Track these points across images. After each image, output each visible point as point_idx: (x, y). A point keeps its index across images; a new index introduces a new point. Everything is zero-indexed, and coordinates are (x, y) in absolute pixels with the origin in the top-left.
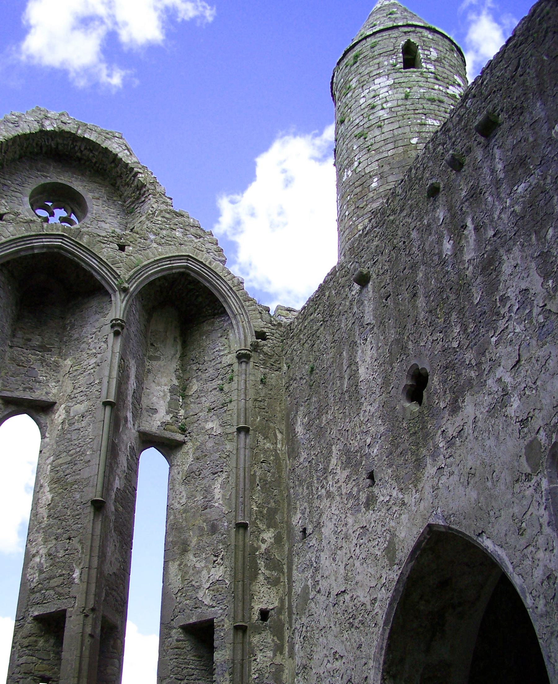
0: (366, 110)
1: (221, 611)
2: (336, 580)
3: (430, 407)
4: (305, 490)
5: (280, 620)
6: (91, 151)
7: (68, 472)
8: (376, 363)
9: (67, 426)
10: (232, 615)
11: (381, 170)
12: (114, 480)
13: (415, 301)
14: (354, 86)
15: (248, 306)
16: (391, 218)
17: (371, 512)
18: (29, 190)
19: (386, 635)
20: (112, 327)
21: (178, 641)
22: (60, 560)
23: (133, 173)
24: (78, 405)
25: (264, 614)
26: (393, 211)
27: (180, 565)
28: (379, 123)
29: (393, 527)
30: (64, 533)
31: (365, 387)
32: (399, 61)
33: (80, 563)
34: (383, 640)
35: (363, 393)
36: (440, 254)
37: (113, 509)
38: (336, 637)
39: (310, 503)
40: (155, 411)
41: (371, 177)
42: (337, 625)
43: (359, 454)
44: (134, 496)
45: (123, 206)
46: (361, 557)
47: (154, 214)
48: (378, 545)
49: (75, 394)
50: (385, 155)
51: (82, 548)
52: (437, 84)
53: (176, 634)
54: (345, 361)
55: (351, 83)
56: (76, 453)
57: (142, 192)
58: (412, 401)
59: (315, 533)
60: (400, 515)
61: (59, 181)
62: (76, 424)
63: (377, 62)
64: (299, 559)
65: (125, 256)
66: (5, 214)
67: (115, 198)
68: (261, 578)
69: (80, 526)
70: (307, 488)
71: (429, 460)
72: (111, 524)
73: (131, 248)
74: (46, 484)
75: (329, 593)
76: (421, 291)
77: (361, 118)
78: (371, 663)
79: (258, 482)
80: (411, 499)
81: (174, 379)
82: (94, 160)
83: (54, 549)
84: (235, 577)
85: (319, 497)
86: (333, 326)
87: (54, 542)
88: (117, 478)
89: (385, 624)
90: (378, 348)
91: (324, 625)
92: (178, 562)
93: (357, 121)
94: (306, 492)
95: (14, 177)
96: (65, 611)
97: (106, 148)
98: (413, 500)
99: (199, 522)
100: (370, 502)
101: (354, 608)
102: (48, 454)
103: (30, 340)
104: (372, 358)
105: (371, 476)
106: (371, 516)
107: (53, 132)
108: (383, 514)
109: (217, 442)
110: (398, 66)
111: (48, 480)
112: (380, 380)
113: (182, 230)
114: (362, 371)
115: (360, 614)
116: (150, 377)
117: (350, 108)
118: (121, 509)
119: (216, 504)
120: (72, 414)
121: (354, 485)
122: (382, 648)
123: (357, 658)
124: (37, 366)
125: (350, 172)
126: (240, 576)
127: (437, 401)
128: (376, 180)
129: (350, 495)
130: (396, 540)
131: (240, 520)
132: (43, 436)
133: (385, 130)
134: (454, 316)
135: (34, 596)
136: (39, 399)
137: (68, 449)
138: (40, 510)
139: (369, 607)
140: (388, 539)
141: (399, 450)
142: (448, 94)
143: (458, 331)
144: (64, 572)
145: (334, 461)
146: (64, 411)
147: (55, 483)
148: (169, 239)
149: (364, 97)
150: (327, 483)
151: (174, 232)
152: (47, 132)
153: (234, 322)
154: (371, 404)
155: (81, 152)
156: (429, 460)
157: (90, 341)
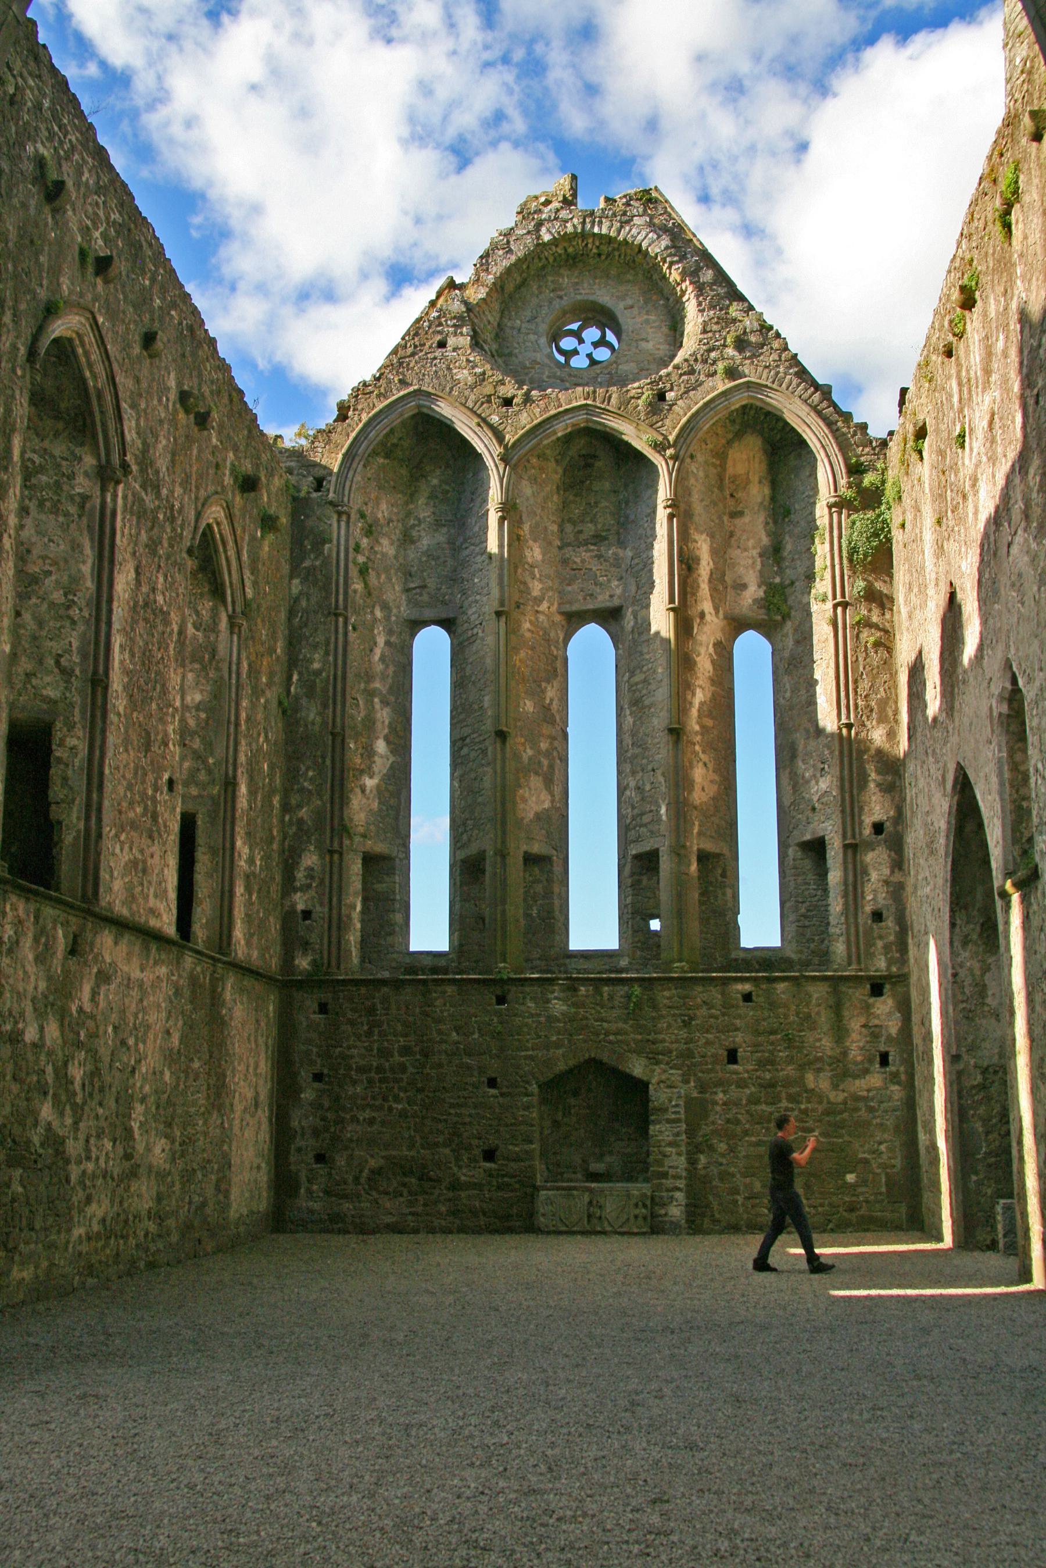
5: (897, 832)
12: (694, 694)
19: (949, 868)
37: (697, 728)
68: (872, 785)
72: (697, 748)
96: (657, 851)
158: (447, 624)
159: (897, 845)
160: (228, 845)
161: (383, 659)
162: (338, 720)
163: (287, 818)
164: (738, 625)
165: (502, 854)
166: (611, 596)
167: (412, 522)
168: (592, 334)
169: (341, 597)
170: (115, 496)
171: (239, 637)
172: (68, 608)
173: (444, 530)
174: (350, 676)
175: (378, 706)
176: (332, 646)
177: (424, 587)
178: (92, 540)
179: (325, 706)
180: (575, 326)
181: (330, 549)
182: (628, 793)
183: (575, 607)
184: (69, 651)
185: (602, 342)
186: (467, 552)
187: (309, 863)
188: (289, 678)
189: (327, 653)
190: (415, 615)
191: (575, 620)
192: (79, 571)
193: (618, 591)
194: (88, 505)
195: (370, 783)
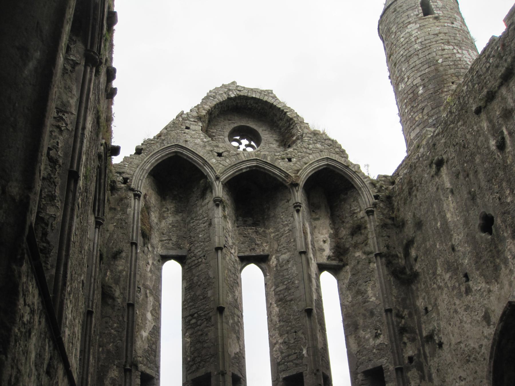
0: (406, 45)
1: (385, 361)
2: (453, 336)
3: (498, 236)
4: (422, 286)
6: (257, 103)
7: (286, 294)
8: (457, 211)
9: (279, 268)
10: (393, 362)
11: (423, 82)
13: (477, 175)
14: (394, 31)
15: (367, 181)
16: (452, 126)
17: (470, 296)
18: (227, 134)
19: (492, 364)
20: (295, 207)
21: (362, 380)
22: (293, 345)
23: (284, 113)
24: (283, 255)
25: (411, 359)
26: (452, 122)
27: (355, 337)
28: (416, 53)
29: (486, 304)
30: (291, 329)
31: (453, 225)
32: (420, 12)
33: (305, 345)
34: (490, 367)
35: (452, 228)
36: (488, 148)
38: (459, 368)
39: (427, 293)
40: (323, 250)
41: (417, 87)
42: (459, 361)
43: (455, 264)
44: (321, 301)
45: (280, 132)
46: (467, 322)
47: (302, 136)
48: (477, 314)
49: (280, 249)
50: (423, 72)
51: (305, 337)
52: (446, 23)
53: (360, 377)
54: (436, 211)
55: (392, 29)
56: (289, 283)
57: (291, 123)
58: (485, 232)
59: (434, 310)
60: (489, 297)
61: (242, 124)
62: (285, 266)
63: (407, 15)
64: (425, 325)
65: (292, 165)
66: (223, 152)
67: (275, 128)
69: (300, 324)
70: (424, 284)
71: (503, 266)
73: (295, 159)
74: (274, 303)
75: (450, 344)
76: (480, 169)
77: (404, 50)
78: (485, 381)
79: (393, 284)
80: (495, 288)
81: (330, 229)
82: (259, 108)
83: (287, 339)
84: (391, 340)
85: (433, 289)
86: (424, 190)
87: (286, 335)
88: (314, 293)
89: (491, 358)
90: (457, 203)
91: (450, 362)
92: (354, 336)
93: (402, 53)
94: (423, 286)
95: (217, 127)
97: (266, 101)
98: (497, 288)
99: (362, 311)
100: (468, 291)
101: (468, 351)
102: (271, 285)
103: (246, 221)
104: (454, 208)
105: (466, 276)
106: (470, 297)
107: (235, 97)
108: (478, 297)
109: (364, 263)
110: (420, 15)
111: (274, 300)
112: (462, 221)
113: (320, 143)
114: (448, 215)
115: (473, 354)
116: (316, 230)
117: (395, 45)
118: (318, 311)
119: (371, 300)
120: (281, 261)
121: (456, 282)
122: (490, 372)
123: (475, 379)
124: (254, 236)
125: (403, 85)
126: (393, 339)
127: (502, 233)
128: (421, 88)
129: (454, 288)
130: (489, 311)
131: (387, 307)
132: (265, 275)
133: (421, 56)
134: (504, 184)
135: (280, 366)
136: (260, 254)
137: (283, 281)
138: (273, 318)
139: (478, 350)
140: (484, 310)
141: (482, 260)
142: (453, 27)
143: (508, 192)
144: (296, 351)
145: (439, 268)
146: (275, 260)
147: (279, 301)
148: (314, 149)
149: (403, 37)
150: (437, 281)
151: (316, 145)
152: (231, 98)
153: (360, 192)
154: (458, 235)
155: (251, 104)
156: (503, 266)
157: (282, 217)
158: (180, 259)
159: (420, 368)
160: (87, 350)
161: (151, 271)
162: (131, 297)
163: (101, 349)
164: (322, 268)
165: (223, 374)
166: (263, 250)
167: (164, 210)
168: (245, 142)
169: (135, 234)
170: (91, 71)
171: (99, 231)
172: (59, 121)
173: (181, 214)
174: (138, 277)
175: (148, 295)
176: (130, 258)
177: (171, 240)
178: (77, 86)
179: (124, 289)
180: (238, 138)
181: (130, 211)
182: (277, 346)
183: (247, 254)
184: (57, 149)
185: (249, 145)
186: (192, 225)
187: (113, 376)
188: (105, 274)
189: (127, 261)
190: (164, 253)
191: (245, 260)
192: (68, 102)
193: (267, 248)
194: (77, 68)
195: (145, 334)
